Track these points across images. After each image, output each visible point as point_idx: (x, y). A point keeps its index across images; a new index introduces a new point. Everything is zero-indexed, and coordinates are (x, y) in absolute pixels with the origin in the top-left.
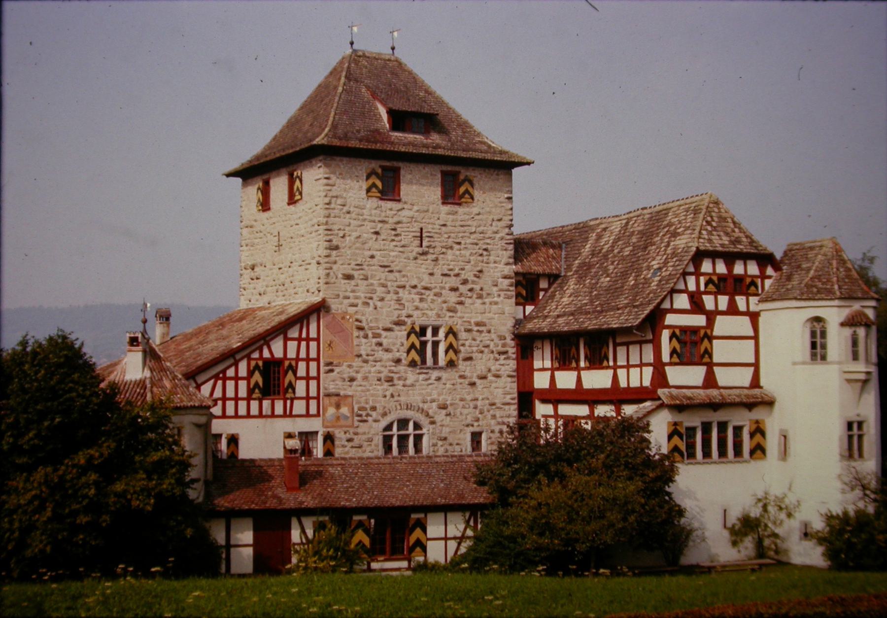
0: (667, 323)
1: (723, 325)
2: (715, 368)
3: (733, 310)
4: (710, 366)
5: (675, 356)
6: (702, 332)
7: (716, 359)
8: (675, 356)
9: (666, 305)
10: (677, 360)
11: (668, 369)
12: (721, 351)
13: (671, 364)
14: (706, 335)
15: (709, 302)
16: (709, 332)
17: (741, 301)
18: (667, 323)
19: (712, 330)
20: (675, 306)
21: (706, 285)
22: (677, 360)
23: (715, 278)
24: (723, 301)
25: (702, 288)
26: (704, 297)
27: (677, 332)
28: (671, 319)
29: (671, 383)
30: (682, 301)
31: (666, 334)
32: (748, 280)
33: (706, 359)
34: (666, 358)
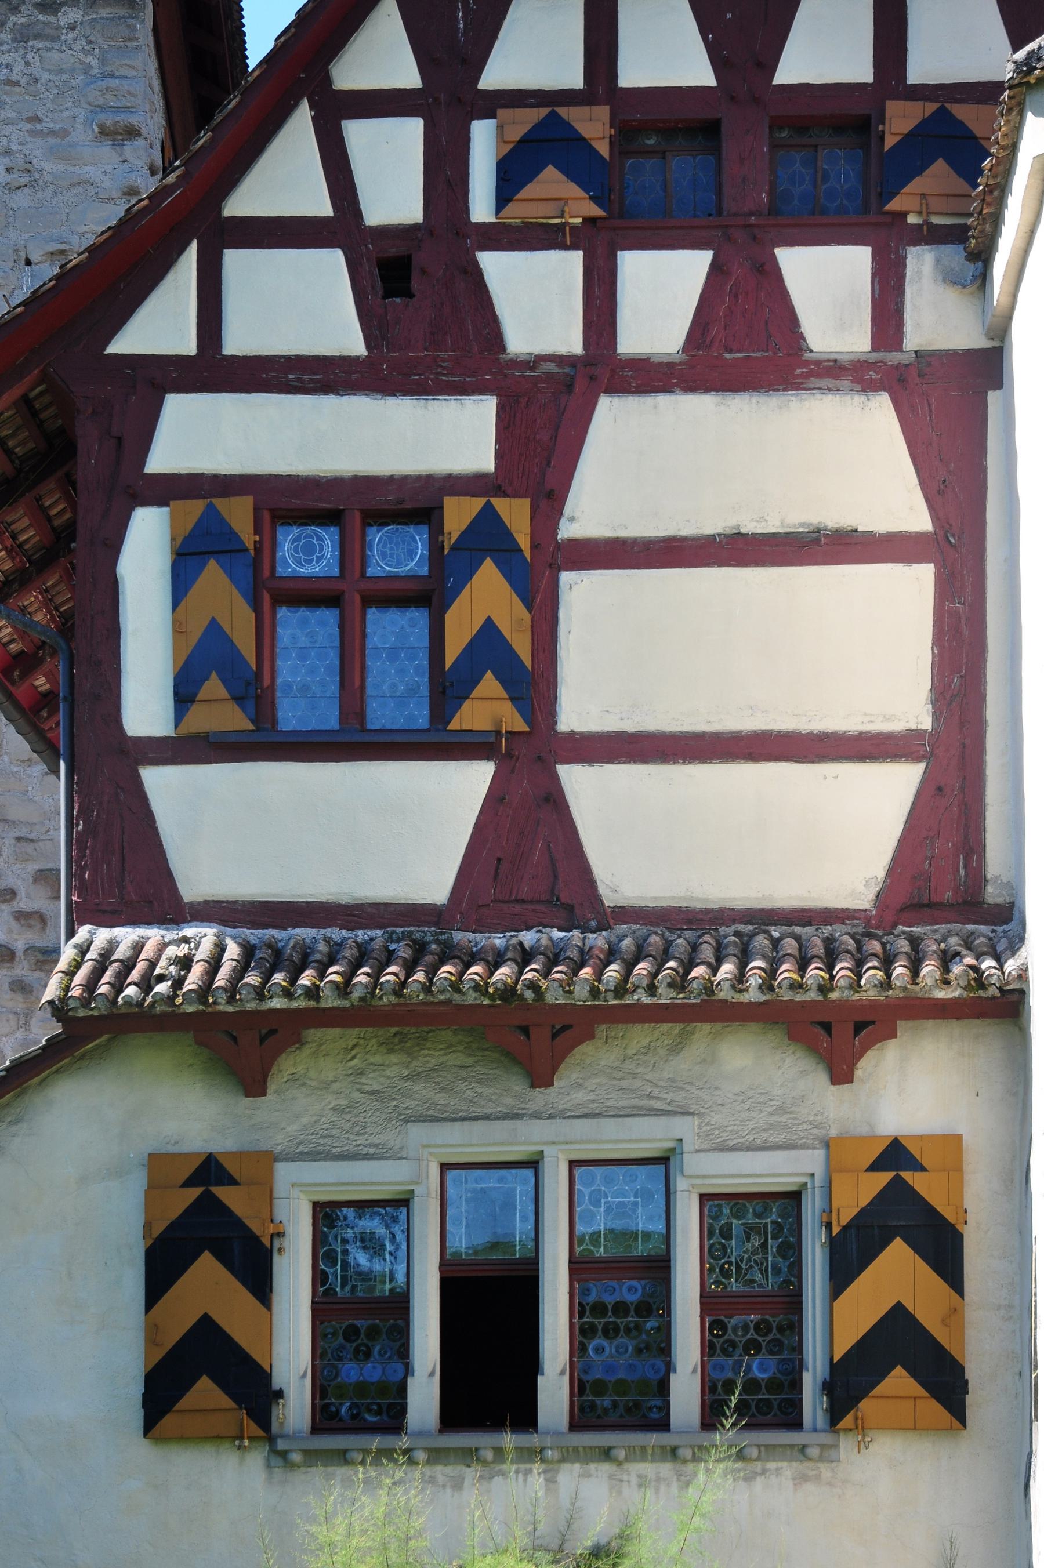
0: (163, 458)
1: (634, 465)
2: (578, 781)
3: (746, 346)
4: (531, 760)
5: (214, 687)
6: (458, 515)
7: (577, 711)
8: (214, 687)
9: (161, 325)
10: (233, 719)
11: (159, 781)
12: (615, 651)
13: (185, 749)
14: (488, 538)
15: (535, 301)
16: (516, 514)
17: (825, 284)
18: (163, 458)
19: (551, 500)
20: (237, 341)
21: (510, 178)
22: (233, 719)
23: (594, 126)
24: (663, 291)
25: (481, 208)
26: (490, 261)
27: (239, 514)
28: (196, 435)
29: (197, 876)
30: (299, 302)
31: (146, 543)
32: (900, 120)
33: (487, 708)
34: (145, 705)
